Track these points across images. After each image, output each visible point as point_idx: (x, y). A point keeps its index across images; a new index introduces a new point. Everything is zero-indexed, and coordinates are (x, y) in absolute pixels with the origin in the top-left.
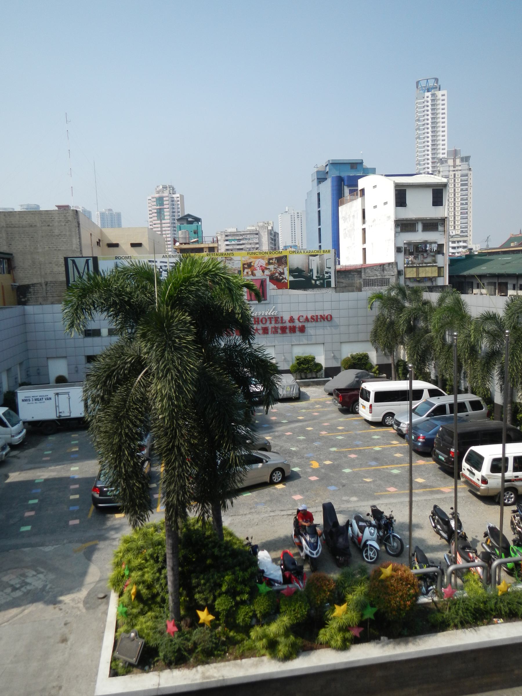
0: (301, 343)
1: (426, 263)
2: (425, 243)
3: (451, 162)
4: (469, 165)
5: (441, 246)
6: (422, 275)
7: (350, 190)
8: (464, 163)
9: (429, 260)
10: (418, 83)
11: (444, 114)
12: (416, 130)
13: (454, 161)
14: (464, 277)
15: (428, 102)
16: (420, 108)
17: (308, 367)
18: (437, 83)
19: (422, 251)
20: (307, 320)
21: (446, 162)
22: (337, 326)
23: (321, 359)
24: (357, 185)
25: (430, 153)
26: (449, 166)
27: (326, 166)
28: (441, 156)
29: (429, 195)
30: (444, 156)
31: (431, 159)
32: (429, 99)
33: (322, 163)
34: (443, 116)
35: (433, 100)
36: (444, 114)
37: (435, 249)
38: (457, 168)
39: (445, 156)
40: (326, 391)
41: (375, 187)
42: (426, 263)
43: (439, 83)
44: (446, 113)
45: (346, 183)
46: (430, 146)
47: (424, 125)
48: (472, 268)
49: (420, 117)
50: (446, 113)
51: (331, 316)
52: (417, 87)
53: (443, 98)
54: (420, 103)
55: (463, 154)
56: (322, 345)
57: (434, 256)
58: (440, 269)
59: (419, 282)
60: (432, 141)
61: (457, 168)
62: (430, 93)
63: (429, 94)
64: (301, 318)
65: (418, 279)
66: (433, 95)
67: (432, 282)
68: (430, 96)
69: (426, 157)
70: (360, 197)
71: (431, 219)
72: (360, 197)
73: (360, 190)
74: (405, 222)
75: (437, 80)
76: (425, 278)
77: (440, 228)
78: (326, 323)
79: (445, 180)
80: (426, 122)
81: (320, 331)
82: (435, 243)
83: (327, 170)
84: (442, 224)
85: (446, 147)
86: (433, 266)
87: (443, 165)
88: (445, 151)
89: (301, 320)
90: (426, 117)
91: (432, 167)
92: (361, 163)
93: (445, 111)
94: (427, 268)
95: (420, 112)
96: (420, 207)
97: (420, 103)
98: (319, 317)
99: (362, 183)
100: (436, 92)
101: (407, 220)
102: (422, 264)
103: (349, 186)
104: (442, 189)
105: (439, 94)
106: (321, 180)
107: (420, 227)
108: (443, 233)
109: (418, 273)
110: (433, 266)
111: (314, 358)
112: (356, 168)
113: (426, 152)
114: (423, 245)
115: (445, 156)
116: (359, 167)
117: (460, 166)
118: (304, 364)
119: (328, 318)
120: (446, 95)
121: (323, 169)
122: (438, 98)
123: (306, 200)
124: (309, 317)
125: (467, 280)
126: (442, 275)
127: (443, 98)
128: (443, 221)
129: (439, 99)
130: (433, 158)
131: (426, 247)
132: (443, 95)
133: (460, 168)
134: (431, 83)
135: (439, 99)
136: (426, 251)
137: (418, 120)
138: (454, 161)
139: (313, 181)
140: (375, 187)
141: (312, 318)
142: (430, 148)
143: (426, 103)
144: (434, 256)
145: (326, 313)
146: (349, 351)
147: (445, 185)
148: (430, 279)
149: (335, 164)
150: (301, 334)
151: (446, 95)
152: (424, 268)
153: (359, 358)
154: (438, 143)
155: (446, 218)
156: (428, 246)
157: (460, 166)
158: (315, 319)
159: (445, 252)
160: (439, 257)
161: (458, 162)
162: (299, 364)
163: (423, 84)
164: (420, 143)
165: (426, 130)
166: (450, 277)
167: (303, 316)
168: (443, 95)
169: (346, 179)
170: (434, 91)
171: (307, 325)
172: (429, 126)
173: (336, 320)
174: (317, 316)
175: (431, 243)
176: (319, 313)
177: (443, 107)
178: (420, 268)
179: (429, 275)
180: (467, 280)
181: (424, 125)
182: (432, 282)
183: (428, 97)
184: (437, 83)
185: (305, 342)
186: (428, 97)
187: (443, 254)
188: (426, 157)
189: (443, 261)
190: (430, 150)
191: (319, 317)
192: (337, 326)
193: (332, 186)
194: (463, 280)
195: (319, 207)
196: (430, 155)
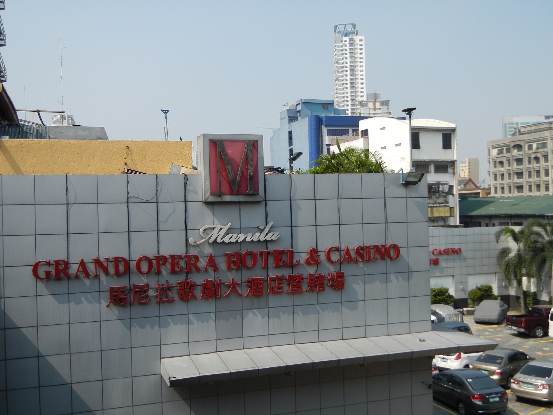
0: (435, 275)
1: (439, 203)
2: (438, 184)
3: (371, 105)
4: (388, 108)
5: (451, 187)
6: (436, 215)
7: (328, 130)
8: (384, 107)
9: (441, 200)
10: (336, 27)
11: (362, 58)
12: (335, 72)
13: (375, 104)
14: (472, 217)
15: (346, 46)
16: (339, 51)
17: (444, 299)
18: (354, 28)
19: (435, 192)
20: (440, 253)
21: (367, 104)
22: (465, 259)
23: (452, 292)
24: (358, 126)
25: (349, 95)
26: (370, 109)
27: (297, 105)
28: (360, 99)
29: (439, 139)
30: (362, 99)
31: (350, 101)
32: (347, 43)
33: (293, 101)
34: (361, 60)
35: (351, 45)
36: (362, 58)
37: (447, 190)
38: (377, 112)
39: (365, 99)
40: (474, 319)
41: (383, 129)
42: (439, 203)
43: (357, 28)
44: (364, 58)
45: (324, 123)
46: (349, 88)
47: (343, 67)
48: (477, 209)
49: (338, 59)
50: (364, 58)
51: (460, 249)
52: (335, 31)
53: (361, 43)
54: (338, 46)
55: (383, 98)
56: (451, 279)
57: (445, 197)
58: (451, 208)
59: (433, 221)
60: (351, 83)
61: (377, 112)
62: (348, 37)
63: (347, 38)
64: (435, 251)
65: (432, 219)
66: (351, 39)
67: (445, 222)
68: (348, 41)
69: (345, 99)
70: (362, 137)
71: (443, 162)
72: (362, 137)
73: (362, 131)
74: (419, 163)
75: (354, 26)
76: (439, 217)
77: (450, 170)
78: (456, 256)
79: (452, 125)
80: (345, 65)
81: (451, 264)
82: (446, 184)
83: (299, 108)
84: (452, 166)
85: (364, 90)
86: (445, 206)
87: (364, 108)
88: (364, 94)
89: (435, 253)
90: (345, 60)
91: (352, 109)
92: (333, 104)
93: (363, 56)
94: (440, 208)
95: (339, 55)
96: (431, 150)
97: (338, 46)
98: (450, 250)
99: (363, 125)
100: (354, 37)
101: (421, 161)
102: (436, 204)
103: (326, 126)
104: (450, 134)
105: (357, 39)
106: (293, 117)
107: (432, 168)
108: (452, 175)
109: (432, 212)
110: (445, 206)
111: (448, 290)
112: (328, 109)
113: (345, 95)
114: (436, 186)
115: (365, 99)
116: (330, 107)
117: (380, 109)
118: (439, 296)
119: (456, 252)
120: (364, 40)
121: (293, 108)
122: (355, 43)
123: (272, 138)
124: (442, 251)
125: (473, 220)
126: (452, 215)
127: (361, 43)
128: (453, 163)
129: (357, 44)
130: (352, 100)
131: (439, 188)
132: (361, 40)
133: (380, 111)
134: (349, 28)
135: (357, 44)
136: (439, 191)
137: (337, 63)
138: (375, 104)
139: (281, 119)
140: (383, 129)
141: (444, 251)
142: (349, 91)
143: (344, 47)
144: (445, 197)
145: (456, 247)
146: (474, 282)
147: (454, 130)
148: (444, 219)
149: (307, 104)
150: (435, 267)
151: (364, 40)
152: (437, 208)
153: (485, 290)
154: (357, 86)
155: (456, 160)
156: (441, 186)
157: (380, 109)
158: (446, 252)
159: (455, 193)
160: (450, 197)
161: (378, 105)
162: (435, 296)
163: (342, 28)
164: (339, 85)
165: (345, 73)
166: (460, 217)
167: (436, 250)
168: (361, 40)
169: (324, 119)
170: (352, 36)
171: (441, 258)
172: (348, 69)
173: (464, 253)
174: (448, 249)
175: (443, 184)
176: (450, 247)
177: (361, 52)
178: (434, 208)
179: (442, 215)
180: (473, 220)
181: (343, 67)
182: (445, 222)
183: (346, 41)
184: (354, 28)
185: (438, 274)
186: (346, 41)
187: (453, 195)
188: (345, 99)
189: (454, 201)
190: (349, 92)
191: (450, 250)
192: (465, 259)
193: (310, 126)
194: (469, 220)
195: (291, 143)
196: (350, 97)
